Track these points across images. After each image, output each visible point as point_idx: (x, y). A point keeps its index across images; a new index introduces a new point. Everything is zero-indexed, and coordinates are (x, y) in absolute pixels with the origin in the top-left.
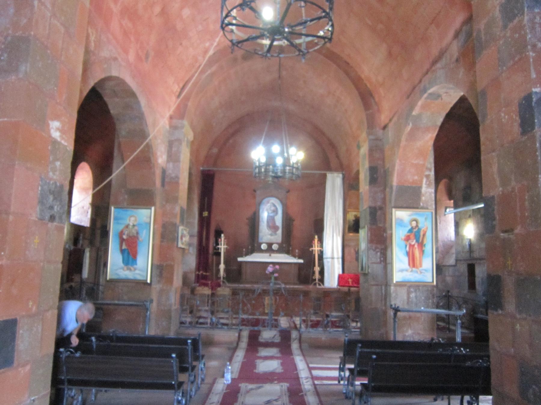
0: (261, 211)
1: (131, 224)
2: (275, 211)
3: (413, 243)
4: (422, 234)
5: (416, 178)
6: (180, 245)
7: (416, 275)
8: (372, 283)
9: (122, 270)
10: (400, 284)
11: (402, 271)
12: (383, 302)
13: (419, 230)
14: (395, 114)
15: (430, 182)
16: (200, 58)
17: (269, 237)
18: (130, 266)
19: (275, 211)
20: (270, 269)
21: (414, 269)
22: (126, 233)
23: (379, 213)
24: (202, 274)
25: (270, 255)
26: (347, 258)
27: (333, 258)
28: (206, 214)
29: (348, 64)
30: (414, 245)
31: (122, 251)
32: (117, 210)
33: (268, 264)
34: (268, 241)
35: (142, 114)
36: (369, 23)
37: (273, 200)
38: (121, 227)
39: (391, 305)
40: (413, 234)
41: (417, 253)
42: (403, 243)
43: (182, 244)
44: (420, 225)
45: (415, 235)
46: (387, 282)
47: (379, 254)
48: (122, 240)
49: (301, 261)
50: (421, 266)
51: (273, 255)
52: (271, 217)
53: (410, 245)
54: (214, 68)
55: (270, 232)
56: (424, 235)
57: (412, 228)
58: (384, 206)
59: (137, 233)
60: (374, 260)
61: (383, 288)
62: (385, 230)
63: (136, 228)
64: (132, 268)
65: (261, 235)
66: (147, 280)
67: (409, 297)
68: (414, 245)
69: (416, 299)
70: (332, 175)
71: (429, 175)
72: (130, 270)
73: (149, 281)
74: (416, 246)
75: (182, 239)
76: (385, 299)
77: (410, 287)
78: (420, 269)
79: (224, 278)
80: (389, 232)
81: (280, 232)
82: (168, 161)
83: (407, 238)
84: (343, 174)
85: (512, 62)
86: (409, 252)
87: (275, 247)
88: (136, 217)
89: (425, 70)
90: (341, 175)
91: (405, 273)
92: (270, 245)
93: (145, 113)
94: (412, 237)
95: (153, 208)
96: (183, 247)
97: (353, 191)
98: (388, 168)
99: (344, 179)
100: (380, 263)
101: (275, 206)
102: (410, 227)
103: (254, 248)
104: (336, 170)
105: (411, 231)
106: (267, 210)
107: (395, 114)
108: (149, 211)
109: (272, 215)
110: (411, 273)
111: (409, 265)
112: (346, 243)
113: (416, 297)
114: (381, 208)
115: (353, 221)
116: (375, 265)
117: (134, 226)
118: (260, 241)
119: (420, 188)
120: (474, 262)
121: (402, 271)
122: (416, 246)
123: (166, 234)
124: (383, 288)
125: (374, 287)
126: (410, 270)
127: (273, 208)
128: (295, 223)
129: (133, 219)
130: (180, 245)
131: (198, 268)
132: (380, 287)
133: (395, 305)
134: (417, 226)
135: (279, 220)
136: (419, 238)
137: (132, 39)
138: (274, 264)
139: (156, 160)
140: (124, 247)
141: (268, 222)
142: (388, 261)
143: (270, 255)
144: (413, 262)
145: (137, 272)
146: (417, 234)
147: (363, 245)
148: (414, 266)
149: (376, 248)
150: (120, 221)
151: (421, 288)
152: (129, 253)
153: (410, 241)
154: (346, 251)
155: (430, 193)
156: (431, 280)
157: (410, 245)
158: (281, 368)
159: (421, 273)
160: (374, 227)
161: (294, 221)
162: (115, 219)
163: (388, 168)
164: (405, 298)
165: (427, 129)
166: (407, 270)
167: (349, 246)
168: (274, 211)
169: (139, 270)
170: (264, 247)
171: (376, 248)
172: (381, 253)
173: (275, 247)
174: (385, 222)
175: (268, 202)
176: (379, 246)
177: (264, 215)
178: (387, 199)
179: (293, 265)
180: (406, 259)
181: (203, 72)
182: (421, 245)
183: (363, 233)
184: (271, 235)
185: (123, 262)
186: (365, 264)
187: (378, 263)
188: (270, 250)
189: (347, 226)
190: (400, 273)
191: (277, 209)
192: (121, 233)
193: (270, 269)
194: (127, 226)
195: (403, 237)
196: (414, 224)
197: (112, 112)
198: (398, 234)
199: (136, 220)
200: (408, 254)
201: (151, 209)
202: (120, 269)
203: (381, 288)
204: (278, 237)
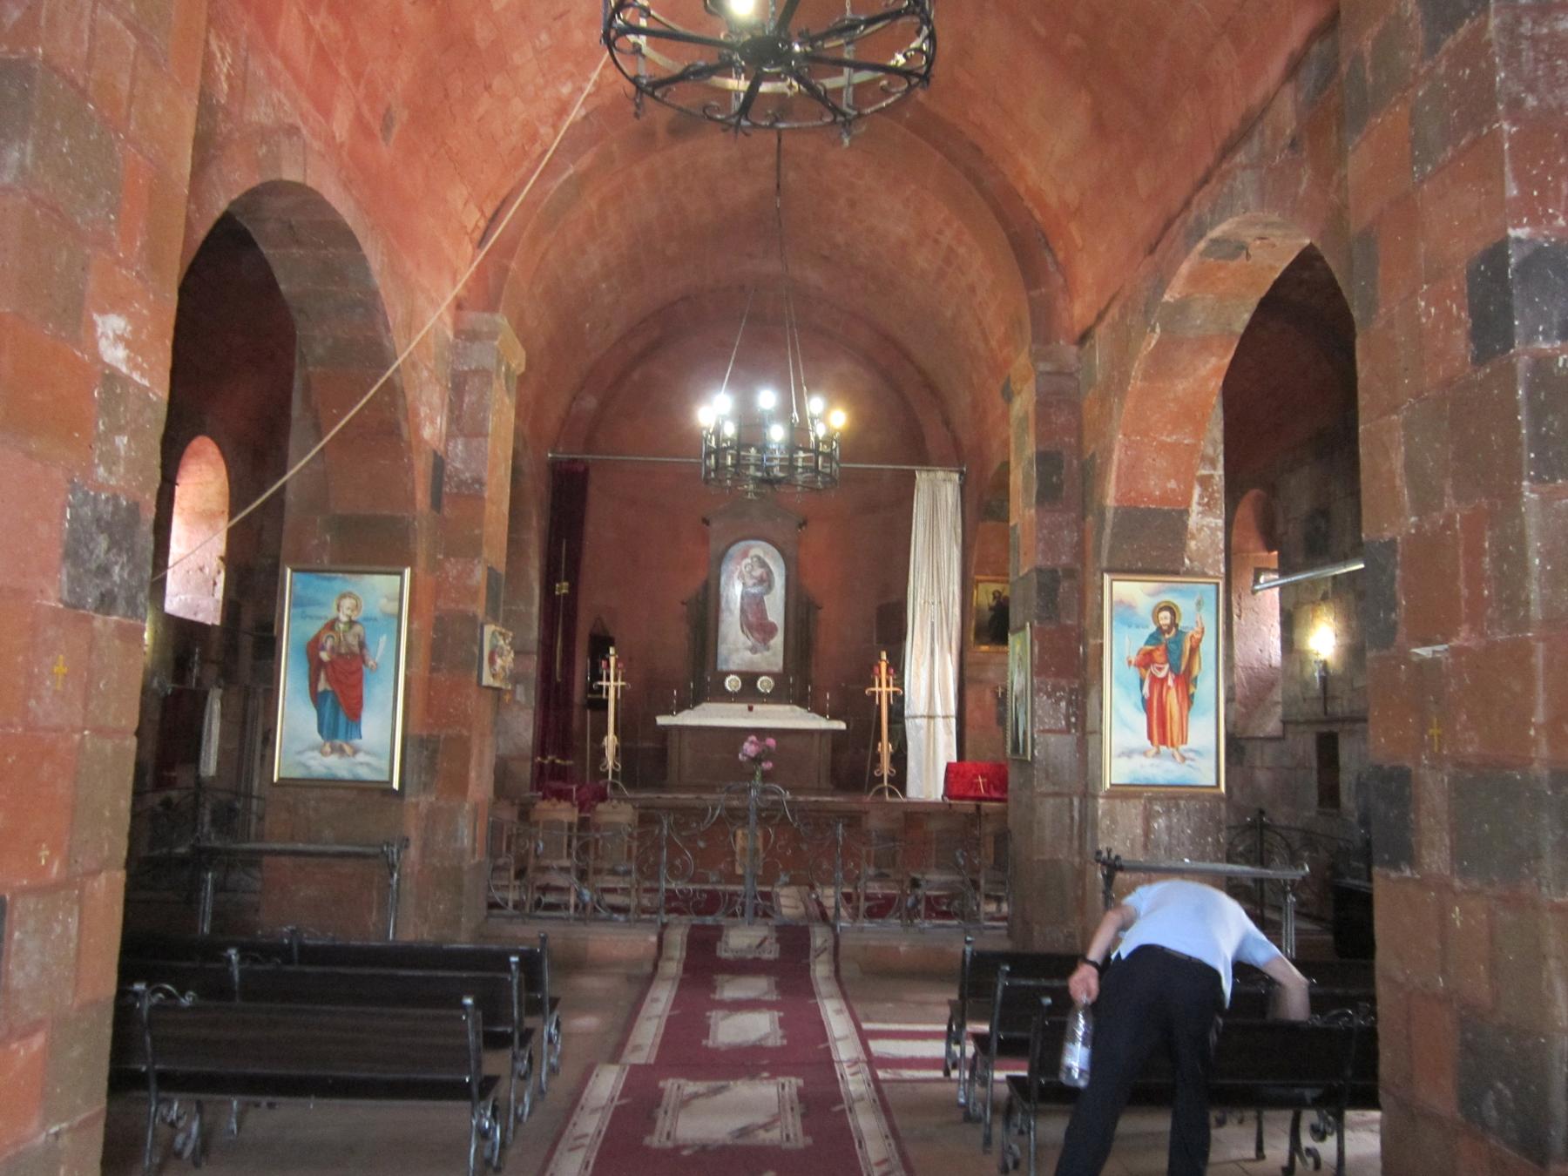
0: (723, 579)
1: (344, 619)
2: (766, 581)
3: (1161, 675)
4: (1188, 646)
5: (1172, 484)
6: (487, 679)
7: (1170, 765)
8: (1043, 789)
9: (316, 754)
10: (1124, 793)
11: (1129, 753)
12: (1076, 843)
13: (1180, 634)
14: (1113, 299)
15: (1211, 497)
16: (544, 130)
17: (748, 654)
18: (338, 742)
19: (766, 581)
20: (750, 748)
21: (1163, 748)
22: (329, 644)
23: (1065, 585)
24: (553, 762)
25: (751, 709)
26: (973, 715)
27: (931, 717)
28: (562, 588)
29: (978, 149)
30: (1165, 679)
31: (317, 698)
32: (298, 576)
34: (744, 668)
35: (375, 294)
36: (1042, 31)
37: (760, 549)
38: (312, 628)
39: (1099, 853)
40: (1162, 647)
41: (1173, 700)
42: (1133, 674)
43: (494, 676)
44: (1182, 624)
45: (1167, 650)
46: (1086, 786)
47: (1063, 704)
48: (316, 666)
49: (842, 725)
50: (1184, 741)
51: (757, 707)
52: (754, 595)
53: (1154, 679)
54: (586, 161)
56: (1194, 650)
57: (1160, 631)
58: (1078, 566)
59: (362, 645)
60: (1050, 723)
61: (1076, 802)
62: (1082, 638)
63: (357, 629)
64: (347, 748)
65: (723, 649)
66: (391, 781)
67: (1147, 831)
68: (1165, 679)
69: (1170, 834)
70: (932, 475)
71: (1211, 476)
72: (341, 751)
73: (396, 785)
74: (1170, 682)
75: (492, 661)
76: (1082, 836)
77: (1150, 800)
78: (1182, 748)
79: (615, 774)
80: (1092, 641)
81: (778, 641)
82: (450, 436)
83: (1146, 660)
84: (961, 473)
85: (1450, 152)
86: (1151, 698)
87: (765, 684)
88: (357, 599)
89: (1200, 172)
90: (956, 476)
91: (1138, 760)
92: (749, 679)
93: (382, 292)
94: (1158, 655)
95: (407, 572)
96: (497, 684)
97: (990, 524)
98: (1093, 455)
100: (1069, 732)
101: (763, 564)
102: (1153, 628)
103: (703, 682)
104: (943, 463)
105: (1154, 638)
106: (741, 576)
107: (1113, 299)
108: (398, 578)
109: (754, 590)
110: (1156, 761)
111: (1150, 737)
112: (967, 673)
113: (1169, 829)
114: (1070, 573)
115: (991, 609)
116: (1052, 738)
117: (351, 623)
118: (722, 667)
119: (1185, 512)
120: (1335, 728)
121: (1129, 753)
122: (1170, 682)
123: (444, 649)
124: (1076, 802)
125: (1051, 801)
126: (1154, 750)
127: (758, 572)
128: (822, 614)
129: (347, 603)
130: (487, 679)
131: (541, 747)
132: (1067, 800)
133: (1109, 851)
134: (1174, 624)
135: (775, 608)
136: (1180, 657)
137: (343, 71)
138: (761, 733)
139: (417, 430)
140: (322, 685)
141: (743, 611)
142: (1089, 726)
143: (751, 709)
144: (1161, 730)
145: (361, 757)
146: (1173, 646)
147: (1018, 680)
148: (1163, 741)
149: (1055, 688)
150: (311, 611)
151: (1182, 803)
152: (336, 707)
153: (1153, 669)
154: (970, 694)
155: (1213, 530)
156: (1213, 782)
157: (1154, 679)
158: (780, 1032)
159: (1184, 759)
160: (1051, 627)
162: (293, 605)
163: (1093, 455)
164: (1139, 831)
165: (1204, 345)
166: (1145, 753)
168: (761, 581)
169: (368, 753)
170: (732, 683)
171: (1055, 688)
172: (1069, 703)
173: (765, 684)
174: (1082, 613)
175: (745, 555)
176: (1063, 682)
177: (734, 591)
178: (1090, 546)
179: (817, 736)
180: (1141, 720)
181: (551, 170)
182: (1186, 680)
183: (1019, 646)
184: (754, 650)
185: (320, 731)
186: (1025, 733)
187: (1060, 732)
188: (749, 693)
190: (1124, 760)
191: (769, 573)
192: (314, 646)
193: (750, 748)
194: (331, 625)
195: (1133, 658)
196: (1165, 618)
197: (282, 287)
198: (1121, 647)
199: (357, 607)
200: (1147, 705)
201: (401, 574)
202: (313, 749)
203: (1071, 803)
204: (773, 656)
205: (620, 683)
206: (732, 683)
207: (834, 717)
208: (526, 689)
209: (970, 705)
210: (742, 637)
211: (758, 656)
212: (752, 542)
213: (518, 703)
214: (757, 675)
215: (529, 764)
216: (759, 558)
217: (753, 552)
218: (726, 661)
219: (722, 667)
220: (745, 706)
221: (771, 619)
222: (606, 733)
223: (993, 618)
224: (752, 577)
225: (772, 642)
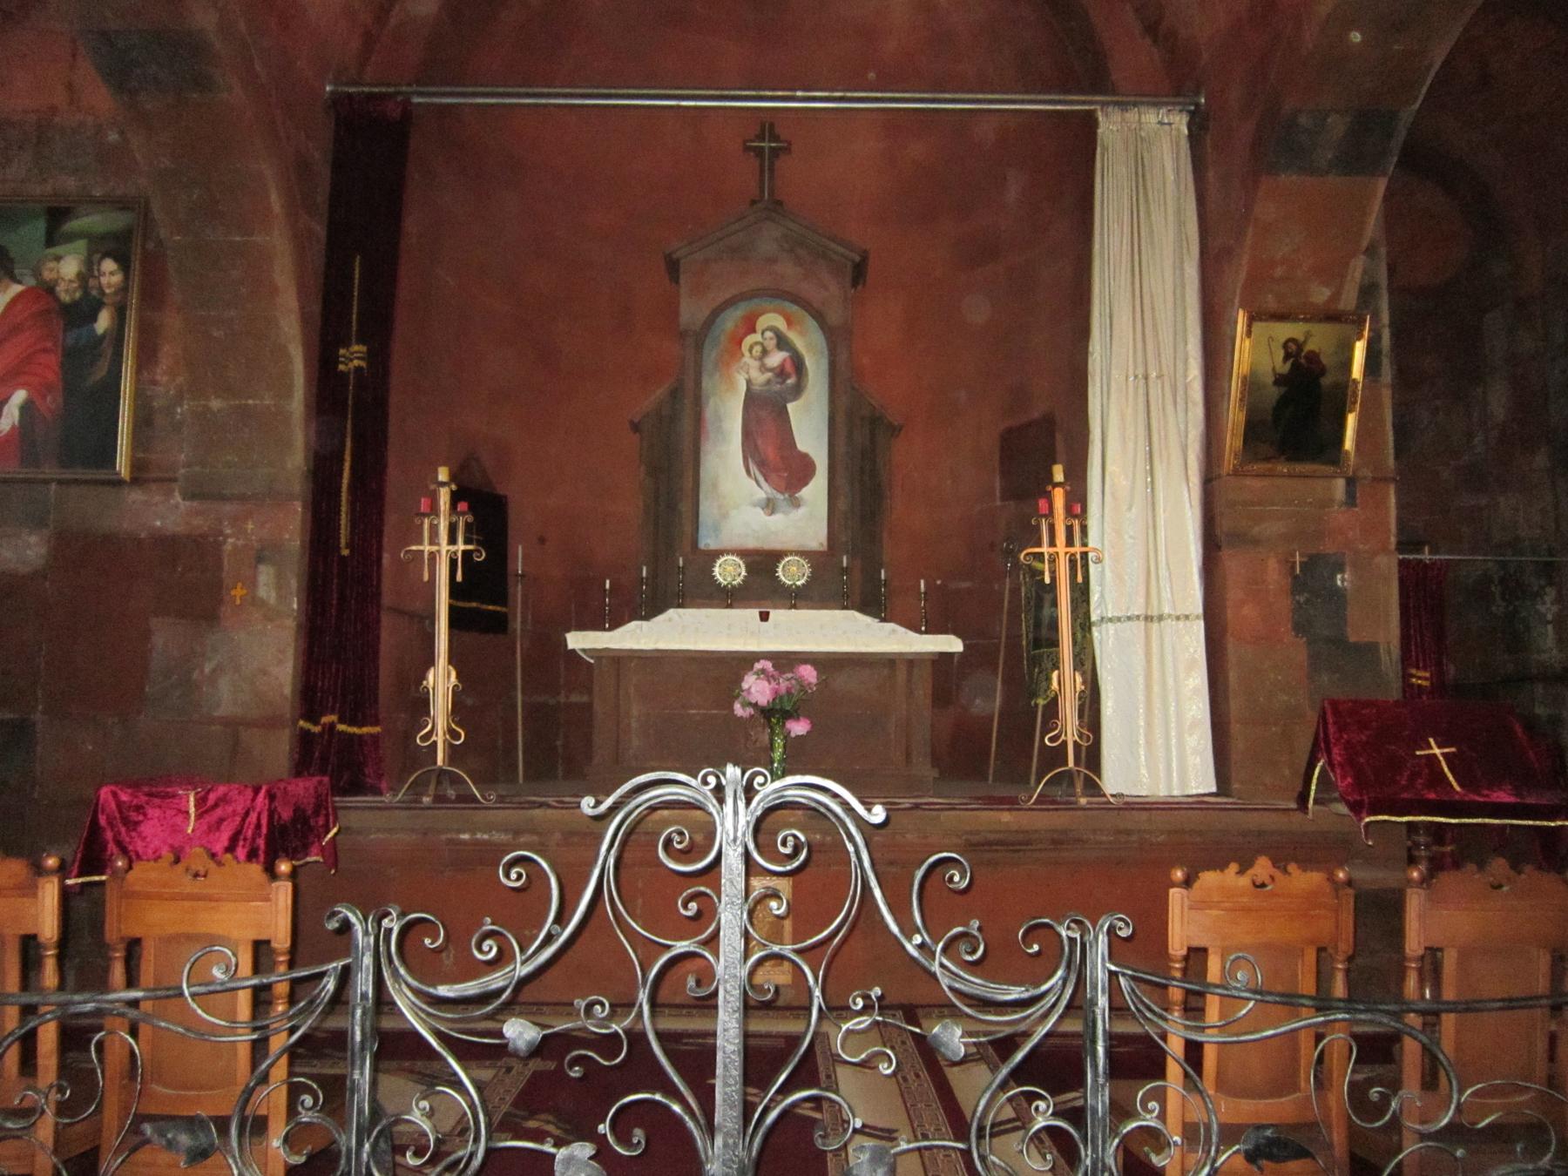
25: (764, 617)
26: (1242, 612)
28: (353, 357)
33: (743, 662)
34: (751, 544)
37: (772, 319)
51: (775, 614)
55: (762, 492)
79: (454, 754)
81: (816, 491)
87: (793, 573)
92: (762, 563)
97: (1288, 179)
99: (1195, 139)
101: (782, 342)
103: (678, 578)
104: (1153, 95)
112: (1224, 525)
115: (1280, 380)
118: (707, 542)
127: (777, 358)
131: (310, 699)
138: (785, 661)
143: (764, 617)
154: (1233, 563)
167: (1256, 542)
168: (781, 373)
170: (729, 571)
173: (793, 573)
188: (762, 584)
189: (1234, 416)
193: (758, 689)
204: (804, 523)
205: (461, 546)
206: (729, 571)
207: (934, 629)
208: (280, 576)
209: (1233, 594)
211: (778, 517)
212: (766, 303)
213: (261, 604)
214: (775, 556)
215: (287, 732)
217: (764, 321)
218: (716, 529)
219: (707, 542)
220: (755, 612)
221: (802, 446)
222: (430, 661)
223: (1283, 403)
224: (763, 368)
225: (805, 493)
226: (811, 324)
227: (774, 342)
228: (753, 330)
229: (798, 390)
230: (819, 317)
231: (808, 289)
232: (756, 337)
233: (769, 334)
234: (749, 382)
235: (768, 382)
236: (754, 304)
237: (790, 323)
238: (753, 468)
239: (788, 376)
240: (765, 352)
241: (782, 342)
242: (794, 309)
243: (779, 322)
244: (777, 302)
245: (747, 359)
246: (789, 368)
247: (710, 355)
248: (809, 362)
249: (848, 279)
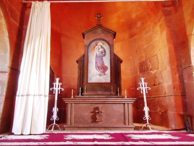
17: (98, 77)
37: (100, 43)
81: (108, 72)
101: (102, 47)
127: (101, 50)
135: (107, 62)
161: (121, 62)
168: (102, 53)
184: (100, 75)
191: (105, 51)
210: (96, 71)
211: (102, 77)
212: (99, 41)
216: (101, 46)
217: (98, 44)
218: (91, 79)
221: (106, 65)
224: (99, 51)
225: (106, 72)
226: (106, 44)
227: (101, 47)
228: (97, 45)
229: (105, 55)
230: (108, 43)
231: (106, 39)
232: (98, 46)
233: (100, 46)
234: (96, 54)
235: (100, 54)
236: (97, 41)
237: (103, 44)
238: (97, 68)
239: (103, 53)
240: (99, 49)
241: (102, 47)
242: (104, 42)
243: (101, 44)
244: (101, 41)
245: (96, 50)
246: (103, 51)
247: (90, 49)
248: (107, 51)
249: (113, 37)
